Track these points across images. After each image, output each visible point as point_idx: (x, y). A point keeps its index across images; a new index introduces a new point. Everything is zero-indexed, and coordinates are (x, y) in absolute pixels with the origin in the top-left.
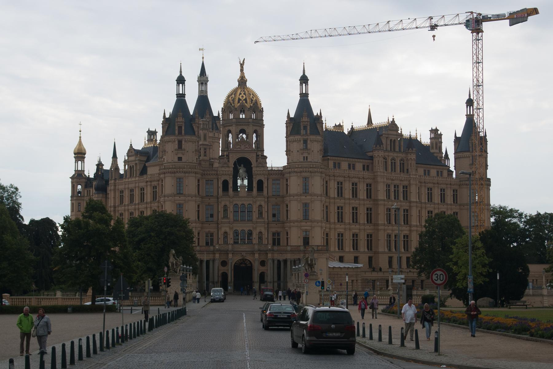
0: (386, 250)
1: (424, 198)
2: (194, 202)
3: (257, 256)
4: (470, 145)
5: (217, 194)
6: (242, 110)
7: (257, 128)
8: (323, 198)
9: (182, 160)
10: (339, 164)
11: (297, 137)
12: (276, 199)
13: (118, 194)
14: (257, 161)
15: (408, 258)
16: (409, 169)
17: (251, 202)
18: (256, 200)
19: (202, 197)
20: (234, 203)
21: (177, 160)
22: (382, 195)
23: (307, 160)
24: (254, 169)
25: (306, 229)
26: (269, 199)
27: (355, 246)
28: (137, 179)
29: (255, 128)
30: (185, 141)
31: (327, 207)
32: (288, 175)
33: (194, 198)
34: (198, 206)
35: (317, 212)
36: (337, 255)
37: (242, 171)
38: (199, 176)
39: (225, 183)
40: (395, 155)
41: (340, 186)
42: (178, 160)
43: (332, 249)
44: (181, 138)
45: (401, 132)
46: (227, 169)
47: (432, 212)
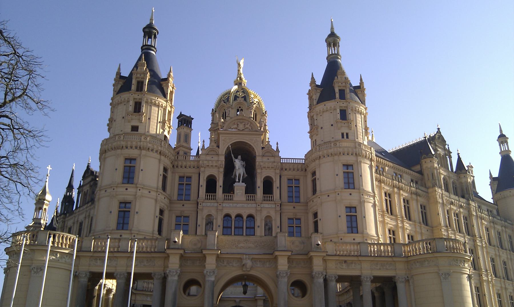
2: (153, 201)
5: (196, 198)
6: (240, 109)
9: (138, 131)
11: (330, 104)
12: (294, 208)
16: (466, 196)
17: (252, 212)
18: (261, 208)
19: (171, 202)
20: (226, 211)
21: (130, 130)
23: (347, 137)
24: (258, 159)
26: (282, 207)
28: (90, 203)
30: (147, 102)
32: (317, 161)
33: (153, 194)
34: (161, 212)
37: (238, 163)
42: (132, 131)
44: (139, 97)
45: (448, 148)
46: (215, 158)
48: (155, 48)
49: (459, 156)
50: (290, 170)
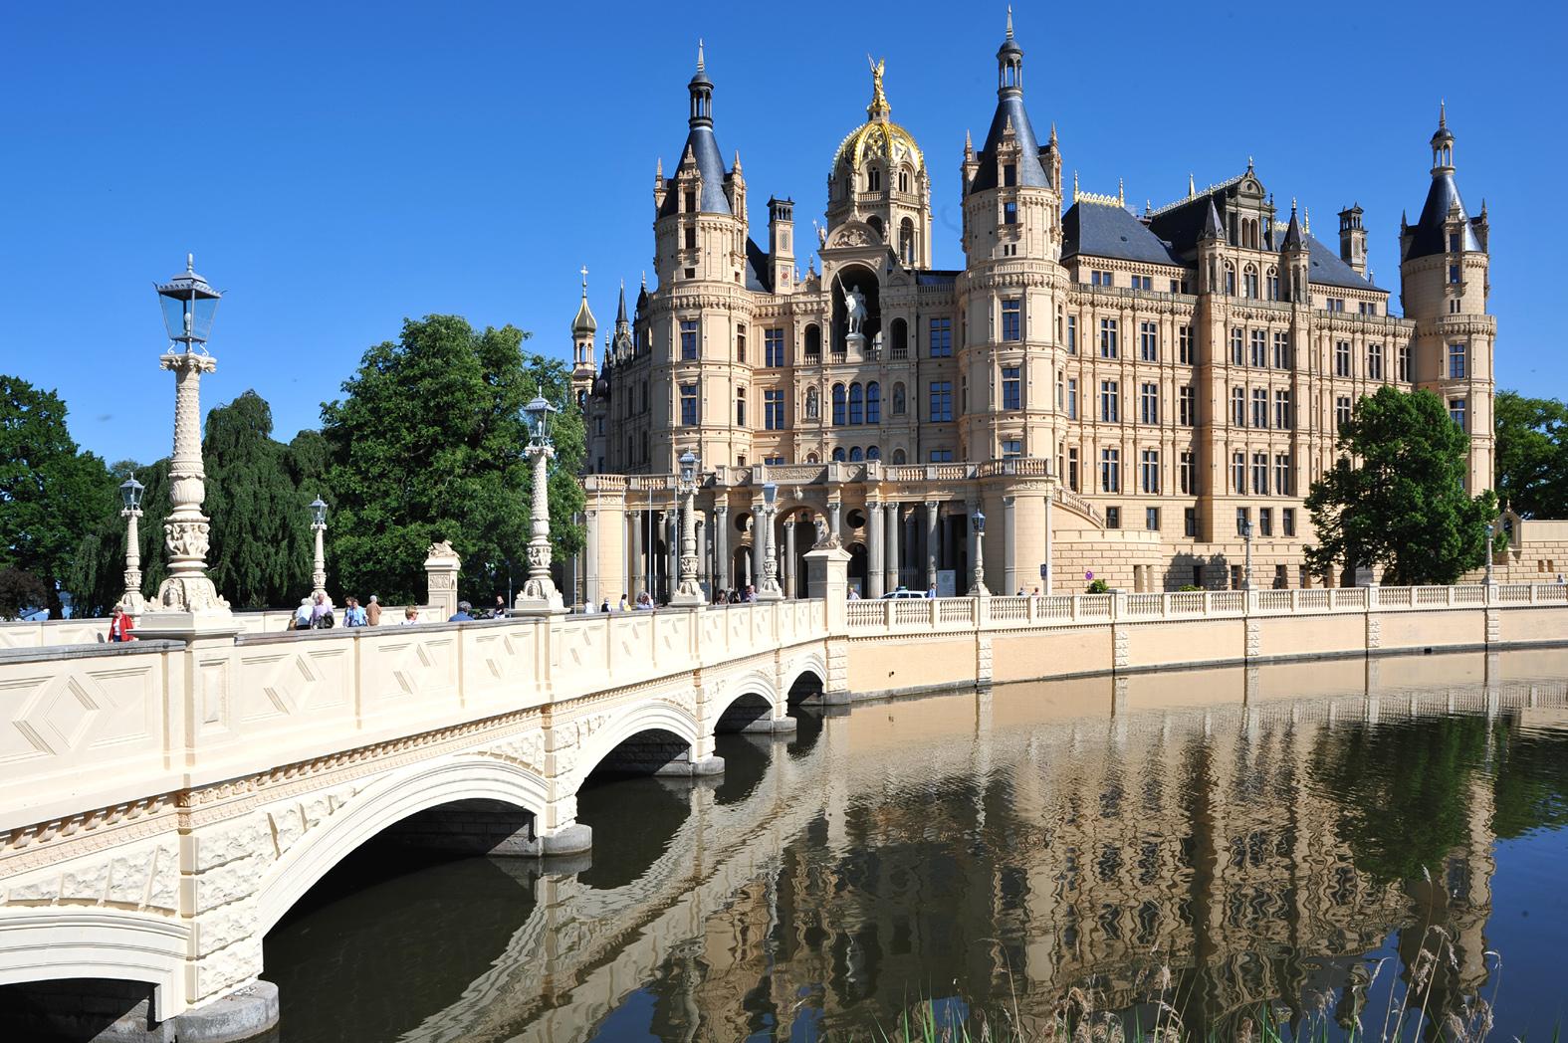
0: (1232, 491)
1: (1328, 365)
3: (835, 497)
4: (1448, 238)
7: (914, 216)
8: (1059, 352)
10: (1109, 275)
13: (626, 395)
14: (889, 272)
15: (1289, 513)
17: (874, 377)
22: (1219, 352)
23: (1014, 253)
24: (883, 293)
25: (1009, 435)
26: (921, 366)
27: (1152, 481)
29: (902, 214)
30: (703, 229)
31: (1073, 381)
34: (741, 392)
35: (1041, 391)
36: (1100, 508)
37: (851, 302)
38: (743, 317)
39: (813, 334)
40: (1256, 256)
41: (1109, 330)
43: (1088, 489)
46: (813, 298)
47: (1347, 400)
48: (709, 119)
49: (1293, 214)
50: (934, 303)
